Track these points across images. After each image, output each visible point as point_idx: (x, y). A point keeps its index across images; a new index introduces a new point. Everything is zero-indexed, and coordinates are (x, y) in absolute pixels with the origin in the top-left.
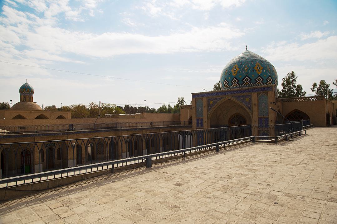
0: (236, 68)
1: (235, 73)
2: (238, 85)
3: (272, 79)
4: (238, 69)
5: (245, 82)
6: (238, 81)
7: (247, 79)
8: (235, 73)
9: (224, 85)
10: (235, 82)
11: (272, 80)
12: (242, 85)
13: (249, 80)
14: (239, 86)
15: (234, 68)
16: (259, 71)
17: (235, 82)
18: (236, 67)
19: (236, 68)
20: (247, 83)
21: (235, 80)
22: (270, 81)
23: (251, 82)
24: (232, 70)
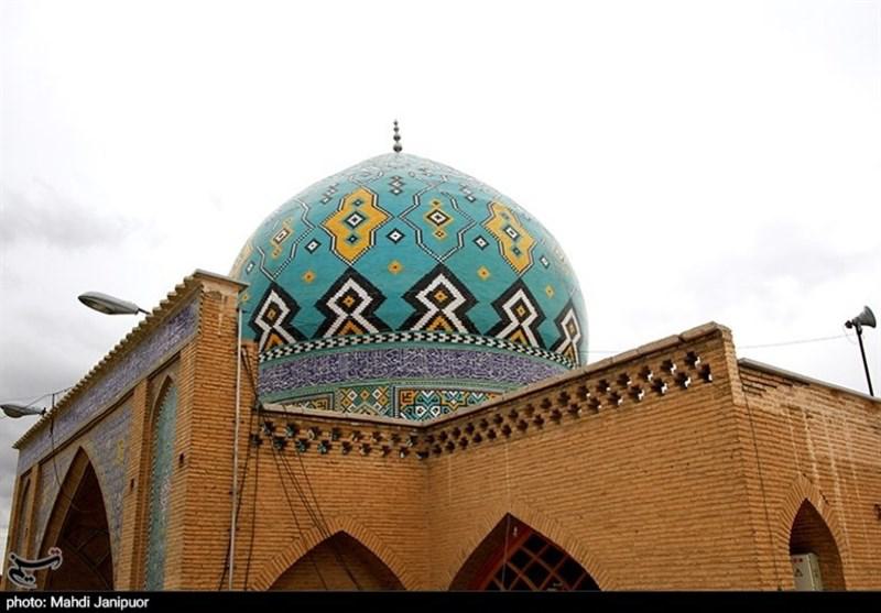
0: (364, 209)
1: (353, 239)
2: (372, 330)
3: (534, 303)
4: (375, 218)
5: (426, 310)
6: (378, 298)
7: (441, 287)
8: (353, 239)
9: (260, 331)
10: (349, 310)
11: (534, 316)
12: (407, 336)
13: (460, 300)
14: (381, 337)
15: (349, 209)
16: (516, 251)
17: (349, 310)
18: (358, 203)
19: (361, 209)
20: (440, 319)
21: (351, 292)
22: (521, 319)
23: (471, 314)
24: (335, 224)
